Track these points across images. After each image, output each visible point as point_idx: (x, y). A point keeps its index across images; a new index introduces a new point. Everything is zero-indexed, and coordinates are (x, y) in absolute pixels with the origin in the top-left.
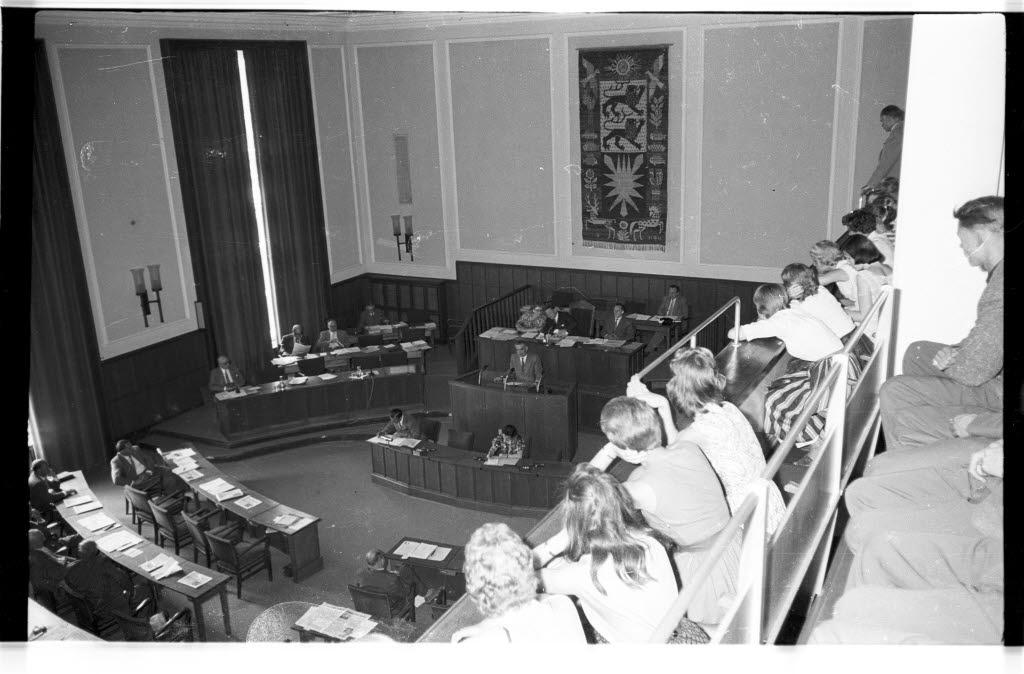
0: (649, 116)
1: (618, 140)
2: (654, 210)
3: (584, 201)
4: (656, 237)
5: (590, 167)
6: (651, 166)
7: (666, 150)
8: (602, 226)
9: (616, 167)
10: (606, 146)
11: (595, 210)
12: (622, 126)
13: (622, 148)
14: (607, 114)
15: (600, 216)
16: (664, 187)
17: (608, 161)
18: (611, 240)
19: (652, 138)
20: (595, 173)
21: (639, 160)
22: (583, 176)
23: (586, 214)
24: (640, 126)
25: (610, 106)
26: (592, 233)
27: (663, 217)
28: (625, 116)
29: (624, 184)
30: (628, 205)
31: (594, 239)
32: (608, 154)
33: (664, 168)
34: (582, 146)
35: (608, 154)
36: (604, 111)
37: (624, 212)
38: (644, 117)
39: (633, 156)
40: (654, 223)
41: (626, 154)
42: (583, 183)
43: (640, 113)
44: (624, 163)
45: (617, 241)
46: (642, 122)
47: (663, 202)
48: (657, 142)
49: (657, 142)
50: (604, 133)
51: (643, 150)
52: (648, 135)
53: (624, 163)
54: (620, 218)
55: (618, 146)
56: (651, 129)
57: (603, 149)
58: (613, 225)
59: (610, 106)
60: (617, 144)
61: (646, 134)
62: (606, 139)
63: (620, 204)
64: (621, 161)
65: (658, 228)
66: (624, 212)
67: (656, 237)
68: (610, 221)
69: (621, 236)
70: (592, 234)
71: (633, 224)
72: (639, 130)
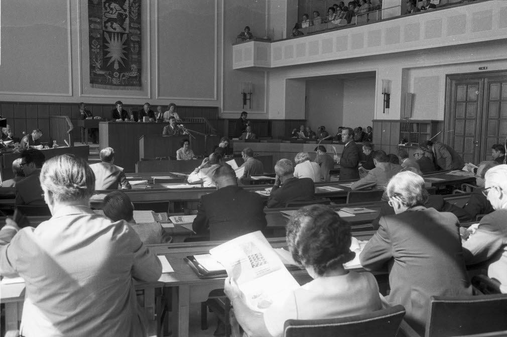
0: (130, 13)
1: (112, 24)
2: (134, 66)
3: (91, 58)
4: (136, 82)
5: (98, 39)
6: (134, 42)
7: (140, 34)
8: (103, 75)
9: (111, 40)
10: (106, 27)
11: (98, 65)
12: (115, 16)
13: (115, 29)
14: (106, 9)
15: (101, 69)
16: (140, 53)
17: (107, 36)
18: (108, 84)
19: (132, 26)
20: (98, 41)
21: (125, 37)
22: (90, 44)
23: (92, 68)
24: (125, 18)
25: (107, 4)
26: (95, 80)
27: (140, 70)
28: (116, 10)
29: (115, 49)
30: (119, 63)
31: (97, 82)
32: (106, 31)
33: (140, 43)
34: (90, 25)
35: (106, 31)
36: (104, 5)
37: (116, 66)
38: (127, 13)
39: (122, 34)
40: (134, 74)
41: (118, 33)
42: (91, 48)
43: (125, 10)
44: (116, 37)
45: (112, 84)
46: (126, 17)
47: (139, 62)
48: (135, 28)
49: (135, 28)
50: (105, 19)
51: (127, 32)
52: (130, 24)
53: (116, 37)
54: (114, 70)
55: (113, 28)
56: (131, 20)
57: (104, 28)
58: (109, 75)
59: (107, 4)
60: (111, 26)
61: (128, 23)
62: (106, 22)
63: (113, 62)
64: (114, 37)
65: (136, 77)
66: (116, 66)
67: (136, 82)
68: (108, 72)
69: (114, 81)
70: (95, 80)
71: (122, 74)
72: (124, 20)
